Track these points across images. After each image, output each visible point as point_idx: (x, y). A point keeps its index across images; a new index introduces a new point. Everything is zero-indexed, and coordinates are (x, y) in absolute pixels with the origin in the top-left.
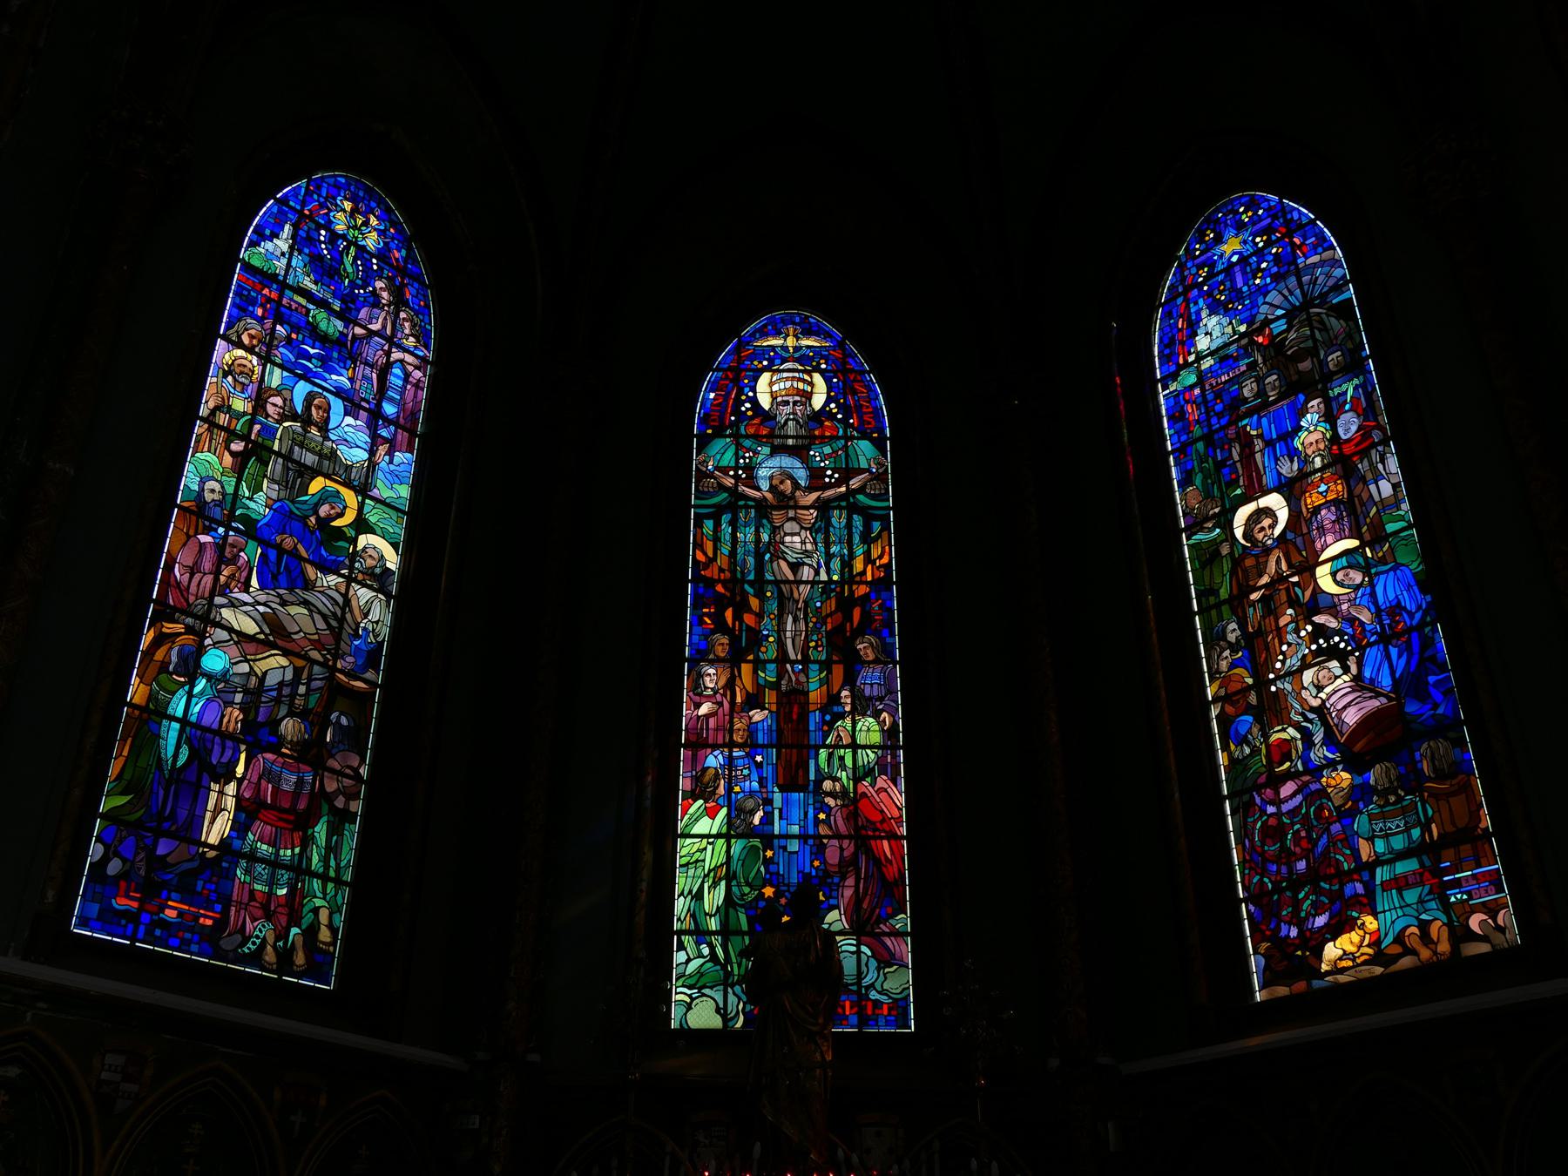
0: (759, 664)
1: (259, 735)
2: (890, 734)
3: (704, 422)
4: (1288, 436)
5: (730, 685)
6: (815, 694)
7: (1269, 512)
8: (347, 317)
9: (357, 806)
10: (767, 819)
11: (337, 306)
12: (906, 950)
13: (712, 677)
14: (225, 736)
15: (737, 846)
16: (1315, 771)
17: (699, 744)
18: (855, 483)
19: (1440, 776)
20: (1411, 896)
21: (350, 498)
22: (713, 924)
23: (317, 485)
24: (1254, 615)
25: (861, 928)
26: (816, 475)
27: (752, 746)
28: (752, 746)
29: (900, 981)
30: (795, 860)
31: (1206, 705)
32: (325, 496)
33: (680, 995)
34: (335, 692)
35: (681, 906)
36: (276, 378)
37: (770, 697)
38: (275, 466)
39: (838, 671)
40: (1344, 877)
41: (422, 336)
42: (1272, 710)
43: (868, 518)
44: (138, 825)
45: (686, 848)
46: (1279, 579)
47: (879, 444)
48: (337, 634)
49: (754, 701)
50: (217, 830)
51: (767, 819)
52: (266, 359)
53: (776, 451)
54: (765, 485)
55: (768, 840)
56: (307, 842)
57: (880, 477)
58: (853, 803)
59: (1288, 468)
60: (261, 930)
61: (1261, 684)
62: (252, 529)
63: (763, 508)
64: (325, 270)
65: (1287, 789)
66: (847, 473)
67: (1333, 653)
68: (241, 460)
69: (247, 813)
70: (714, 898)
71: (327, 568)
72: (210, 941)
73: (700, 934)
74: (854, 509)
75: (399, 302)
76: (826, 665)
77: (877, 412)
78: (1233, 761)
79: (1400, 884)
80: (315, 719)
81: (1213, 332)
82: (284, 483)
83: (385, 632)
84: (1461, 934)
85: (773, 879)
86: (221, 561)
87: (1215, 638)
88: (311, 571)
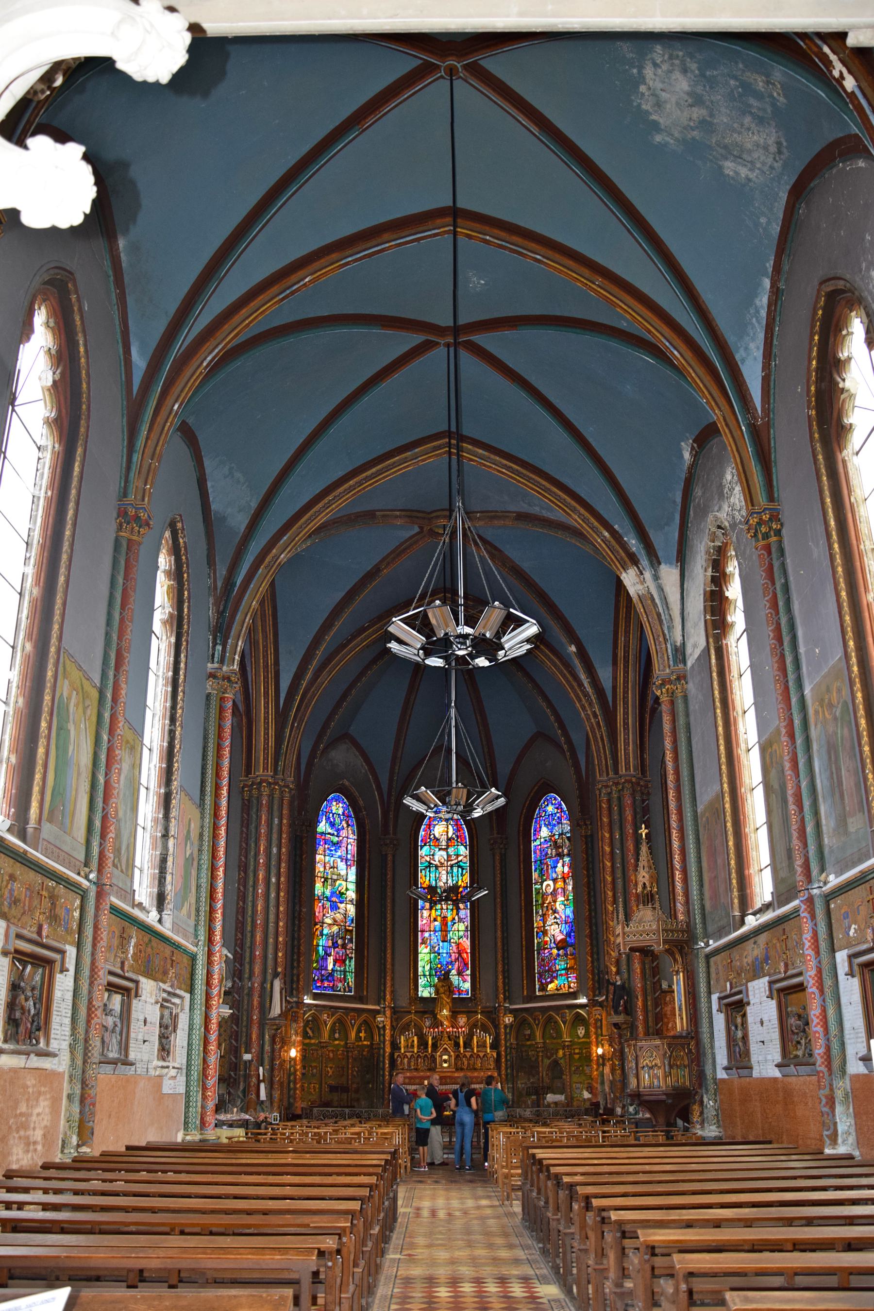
0: (436, 910)
1: (335, 945)
2: (467, 927)
3: (422, 841)
4: (555, 867)
5: (430, 915)
6: (450, 918)
7: (548, 885)
8: (338, 836)
9: (353, 955)
10: (439, 949)
11: (336, 833)
12: (469, 978)
13: (426, 913)
14: (329, 947)
15: (432, 955)
16: (551, 949)
17: (423, 931)
18: (460, 859)
19: (571, 955)
20: (563, 978)
21: (344, 883)
22: (427, 973)
23: (338, 883)
24: (545, 909)
25: (460, 973)
26: (449, 856)
27: (435, 931)
28: (435, 931)
29: (467, 986)
30: (445, 958)
31: (533, 928)
32: (340, 885)
33: (420, 989)
34: (347, 931)
35: (420, 969)
36: (327, 858)
37: (439, 919)
38: (330, 881)
39: (455, 911)
40: (554, 972)
41: (353, 833)
42: (545, 933)
43: (463, 869)
44: (318, 969)
45: (420, 956)
46: (550, 903)
47: (466, 847)
48: (345, 918)
49: (435, 920)
50: (330, 967)
51: (439, 949)
52: (325, 856)
53: (440, 849)
54: (437, 859)
55: (439, 954)
56: (345, 965)
57: (465, 857)
58: (458, 945)
59: (554, 876)
60: (340, 985)
61: (544, 926)
62: (328, 899)
63: (437, 867)
64: (332, 825)
65: (546, 951)
66: (458, 856)
67: (557, 923)
68: (323, 882)
69: (335, 961)
70: (427, 968)
71: (341, 902)
72: (333, 988)
73: (425, 976)
74: (459, 867)
75: (348, 825)
76: (452, 910)
77: (465, 837)
78: (538, 943)
79: (561, 975)
80: (343, 938)
81: (545, 832)
82: (331, 885)
83: (354, 914)
84: (569, 987)
85: (440, 963)
86: (324, 908)
87: (537, 913)
88: (339, 905)
